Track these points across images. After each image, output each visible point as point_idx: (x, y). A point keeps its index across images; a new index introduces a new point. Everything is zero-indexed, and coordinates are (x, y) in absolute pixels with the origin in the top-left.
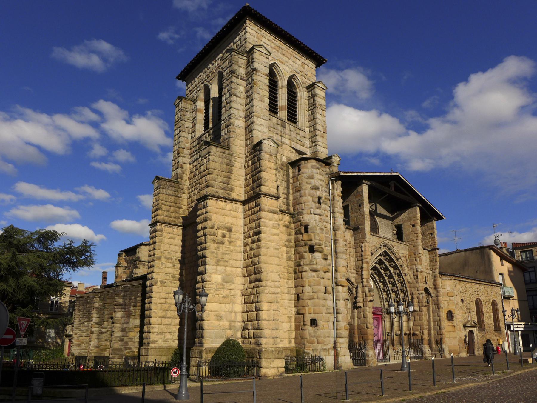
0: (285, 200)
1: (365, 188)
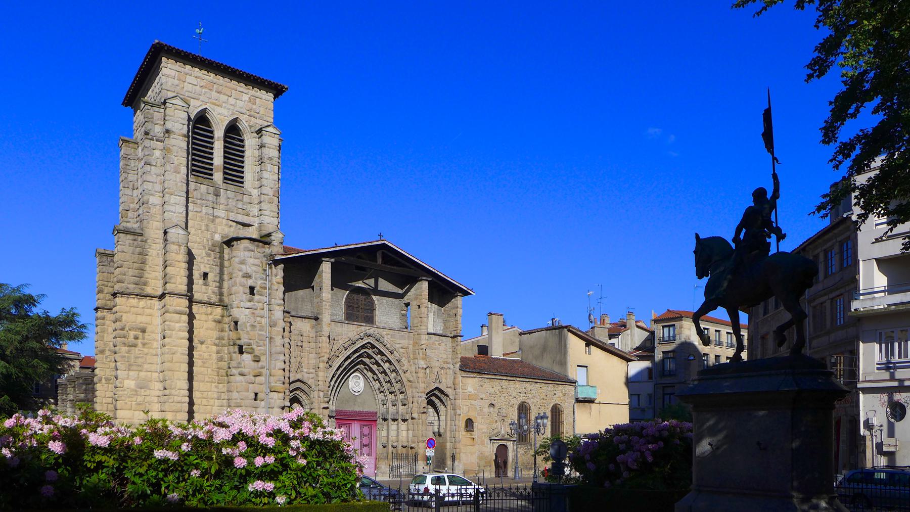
0: (216, 290)
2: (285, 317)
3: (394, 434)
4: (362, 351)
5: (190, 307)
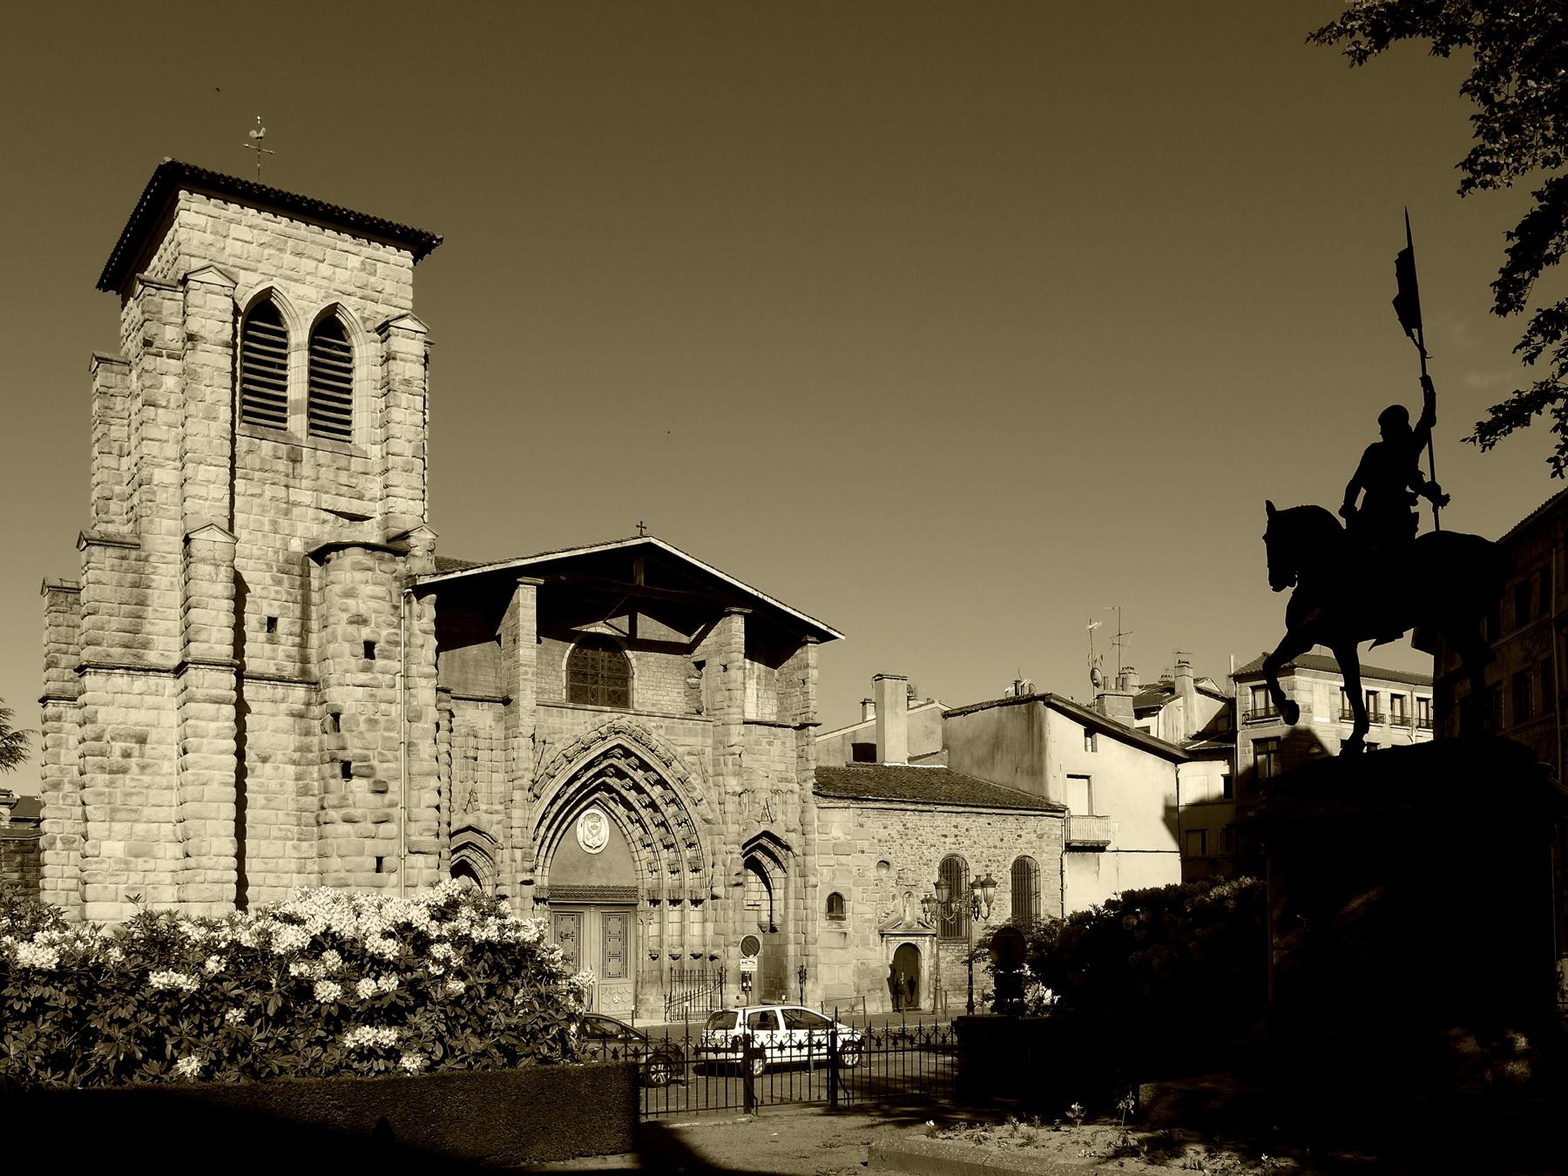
0: (294, 651)
1: (526, 598)
2: (439, 701)
3: (687, 929)
4: (605, 763)
5: (239, 689)
